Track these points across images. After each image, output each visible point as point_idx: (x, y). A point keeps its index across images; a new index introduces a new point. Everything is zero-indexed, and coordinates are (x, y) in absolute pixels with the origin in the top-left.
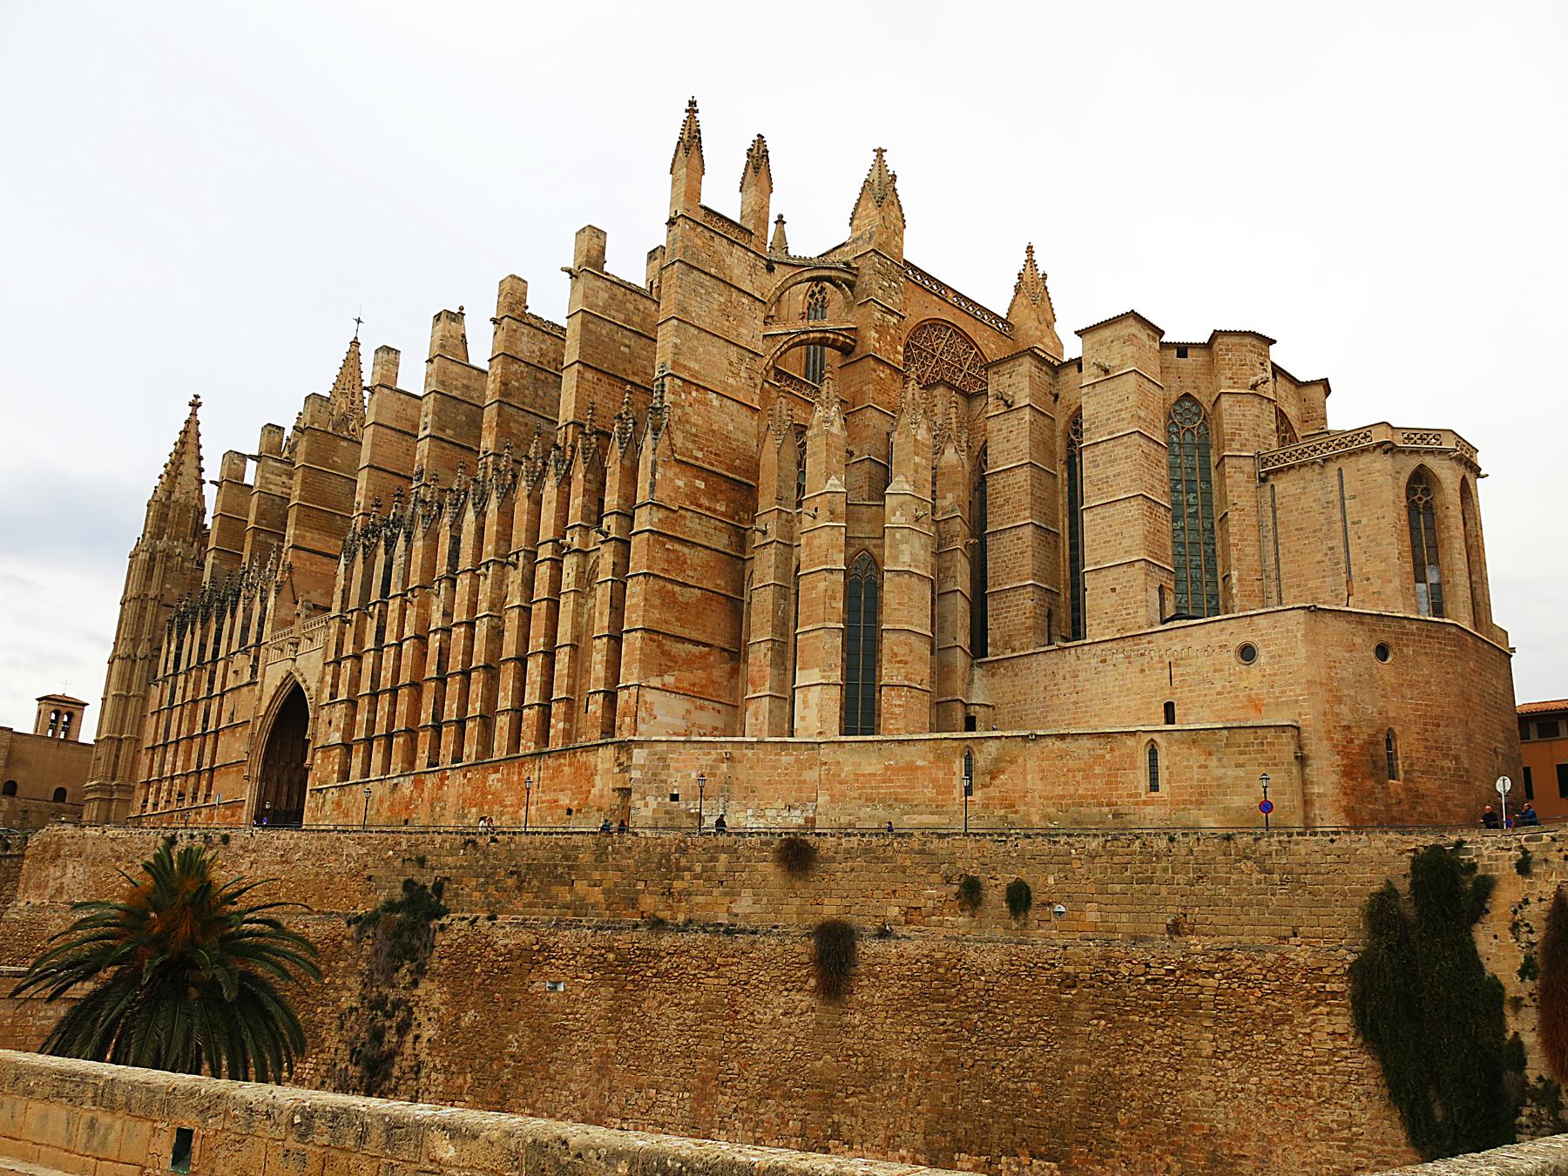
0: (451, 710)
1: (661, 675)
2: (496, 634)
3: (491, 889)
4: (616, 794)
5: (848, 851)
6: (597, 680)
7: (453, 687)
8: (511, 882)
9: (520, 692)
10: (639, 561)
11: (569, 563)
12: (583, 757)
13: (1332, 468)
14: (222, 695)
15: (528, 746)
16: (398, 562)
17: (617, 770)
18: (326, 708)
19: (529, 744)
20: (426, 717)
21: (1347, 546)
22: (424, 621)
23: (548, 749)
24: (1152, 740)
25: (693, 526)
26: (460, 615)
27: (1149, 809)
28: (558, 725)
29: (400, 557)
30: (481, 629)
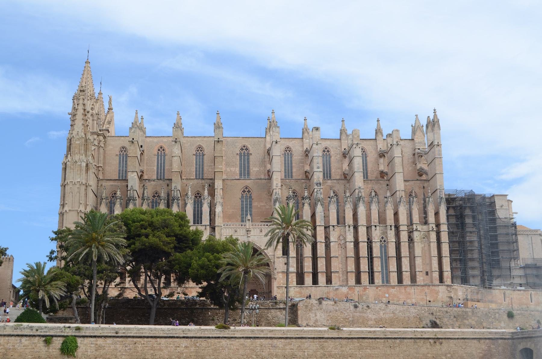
3: (450, 321)
4: (448, 298)
5: (518, 314)
6: (435, 268)
8: (455, 319)
11: (416, 235)
12: (433, 288)
13: (530, 236)
17: (447, 292)
18: (281, 258)
19: (408, 282)
21: (533, 253)
23: (417, 284)
24: (531, 293)
27: (532, 306)
28: (420, 278)
29: (321, 212)
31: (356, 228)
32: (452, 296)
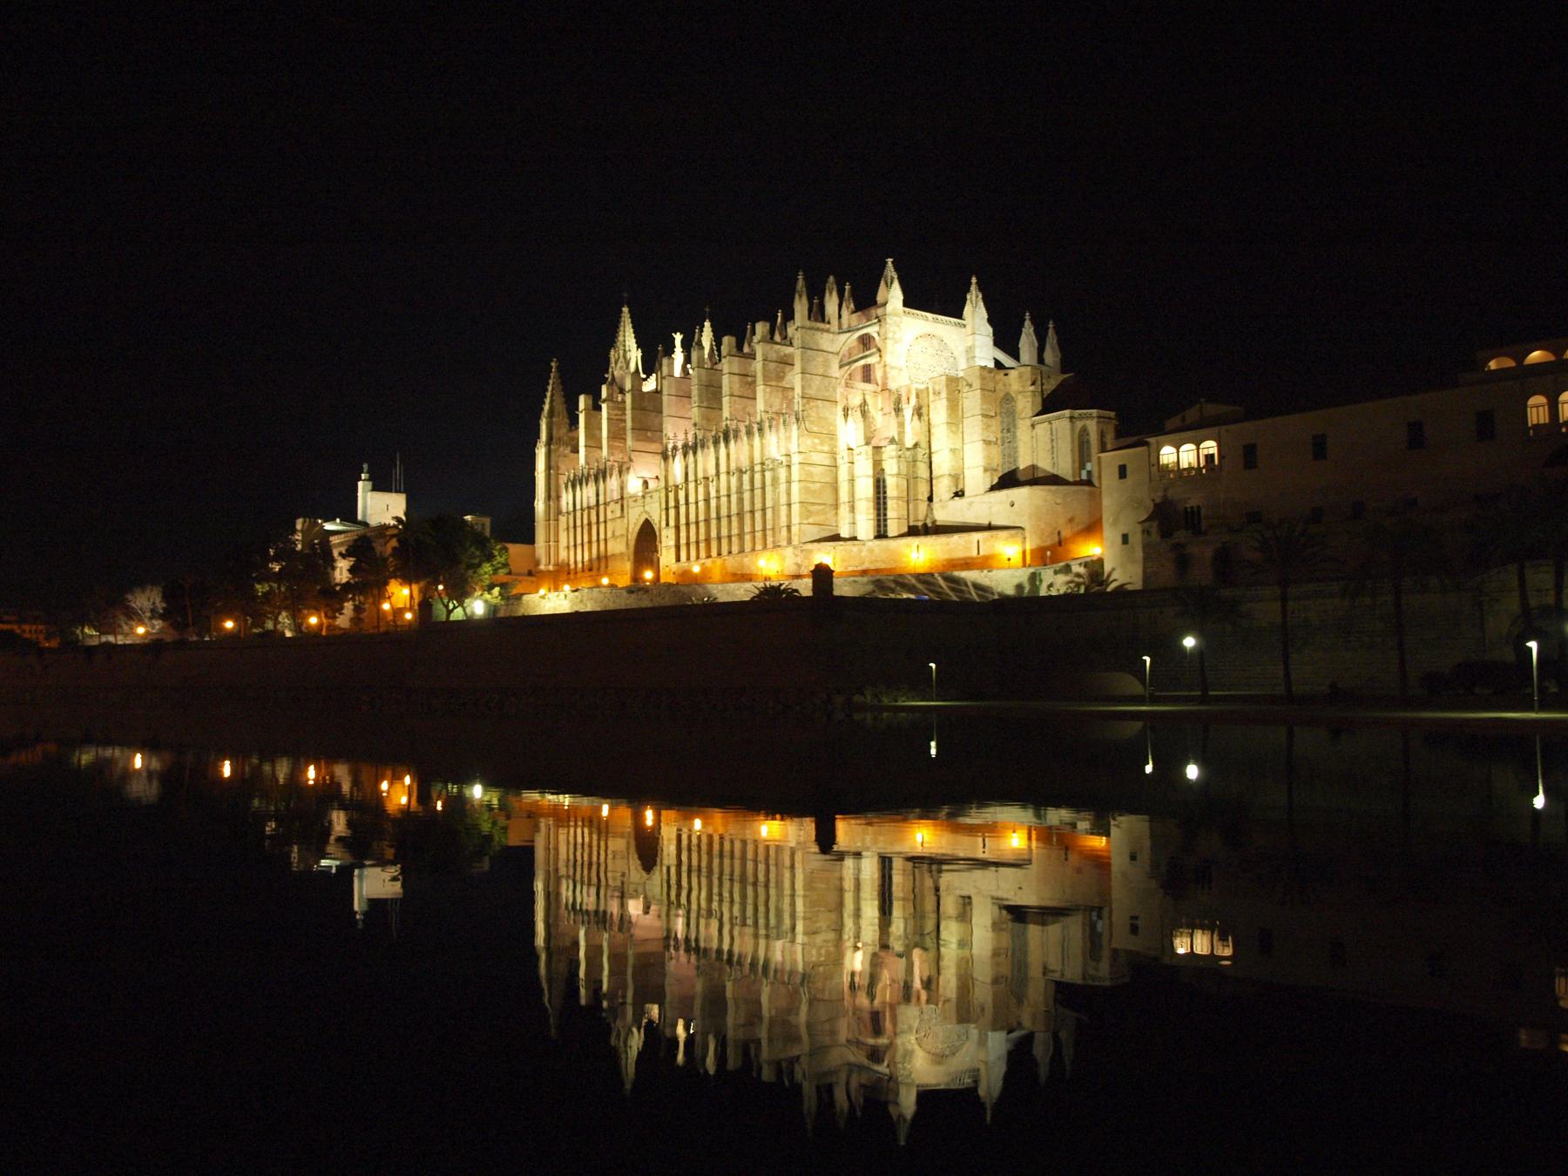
0: (724, 532)
1: (807, 519)
2: (741, 500)
7: (724, 522)
9: (753, 525)
10: (795, 476)
11: (768, 475)
14: (605, 522)
15: (759, 546)
16: (691, 467)
20: (714, 534)
22: (707, 494)
25: (817, 458)
26: (723, 492)
28: (770, 539)
30: (734, 498)
31: (719, 479)
32: (799, 562)
